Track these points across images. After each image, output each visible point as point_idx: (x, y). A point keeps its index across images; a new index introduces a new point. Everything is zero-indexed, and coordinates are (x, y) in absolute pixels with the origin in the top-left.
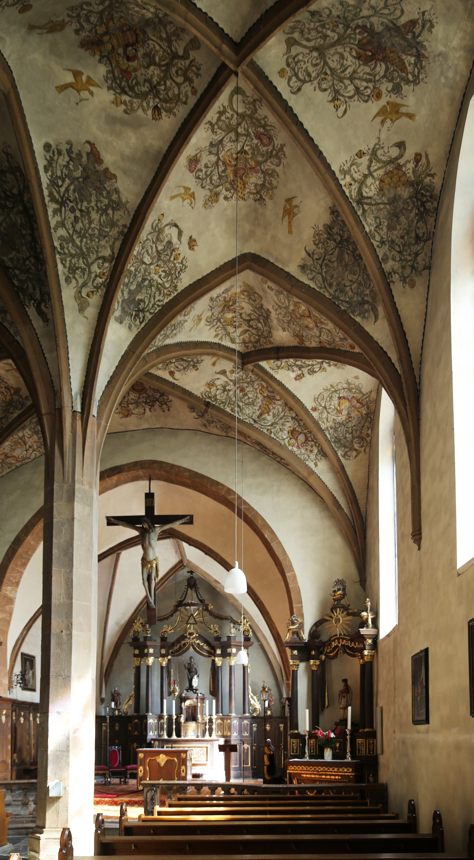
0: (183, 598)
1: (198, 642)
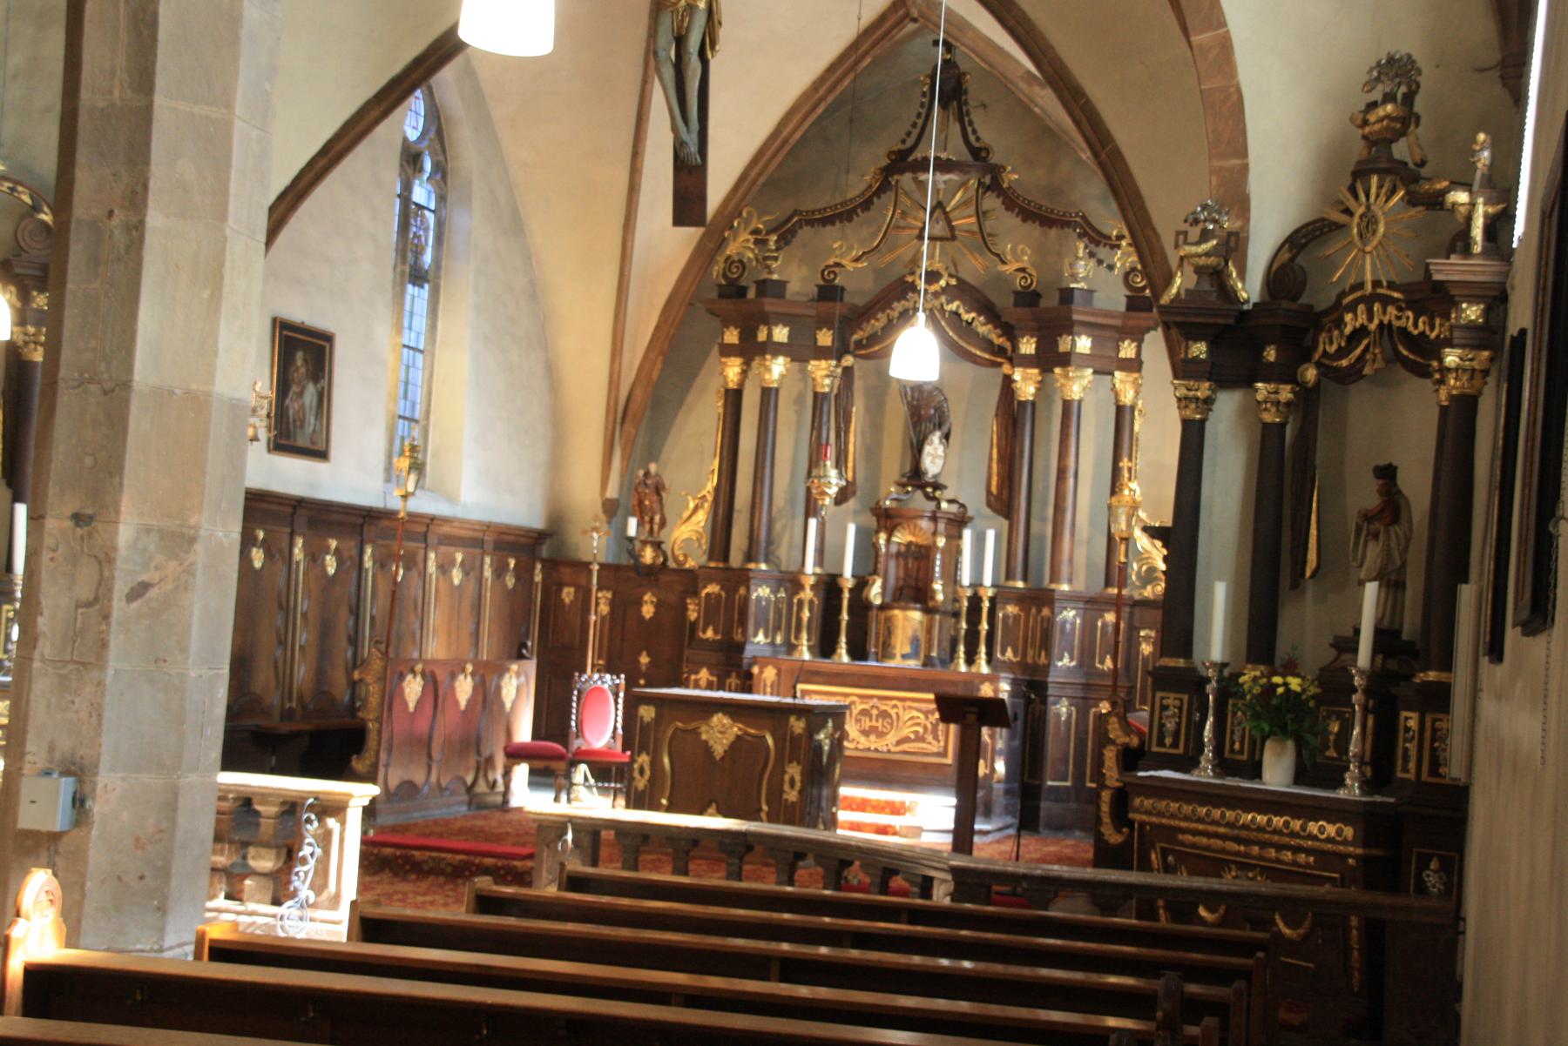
0: (910, 143)
1: (953, 306)
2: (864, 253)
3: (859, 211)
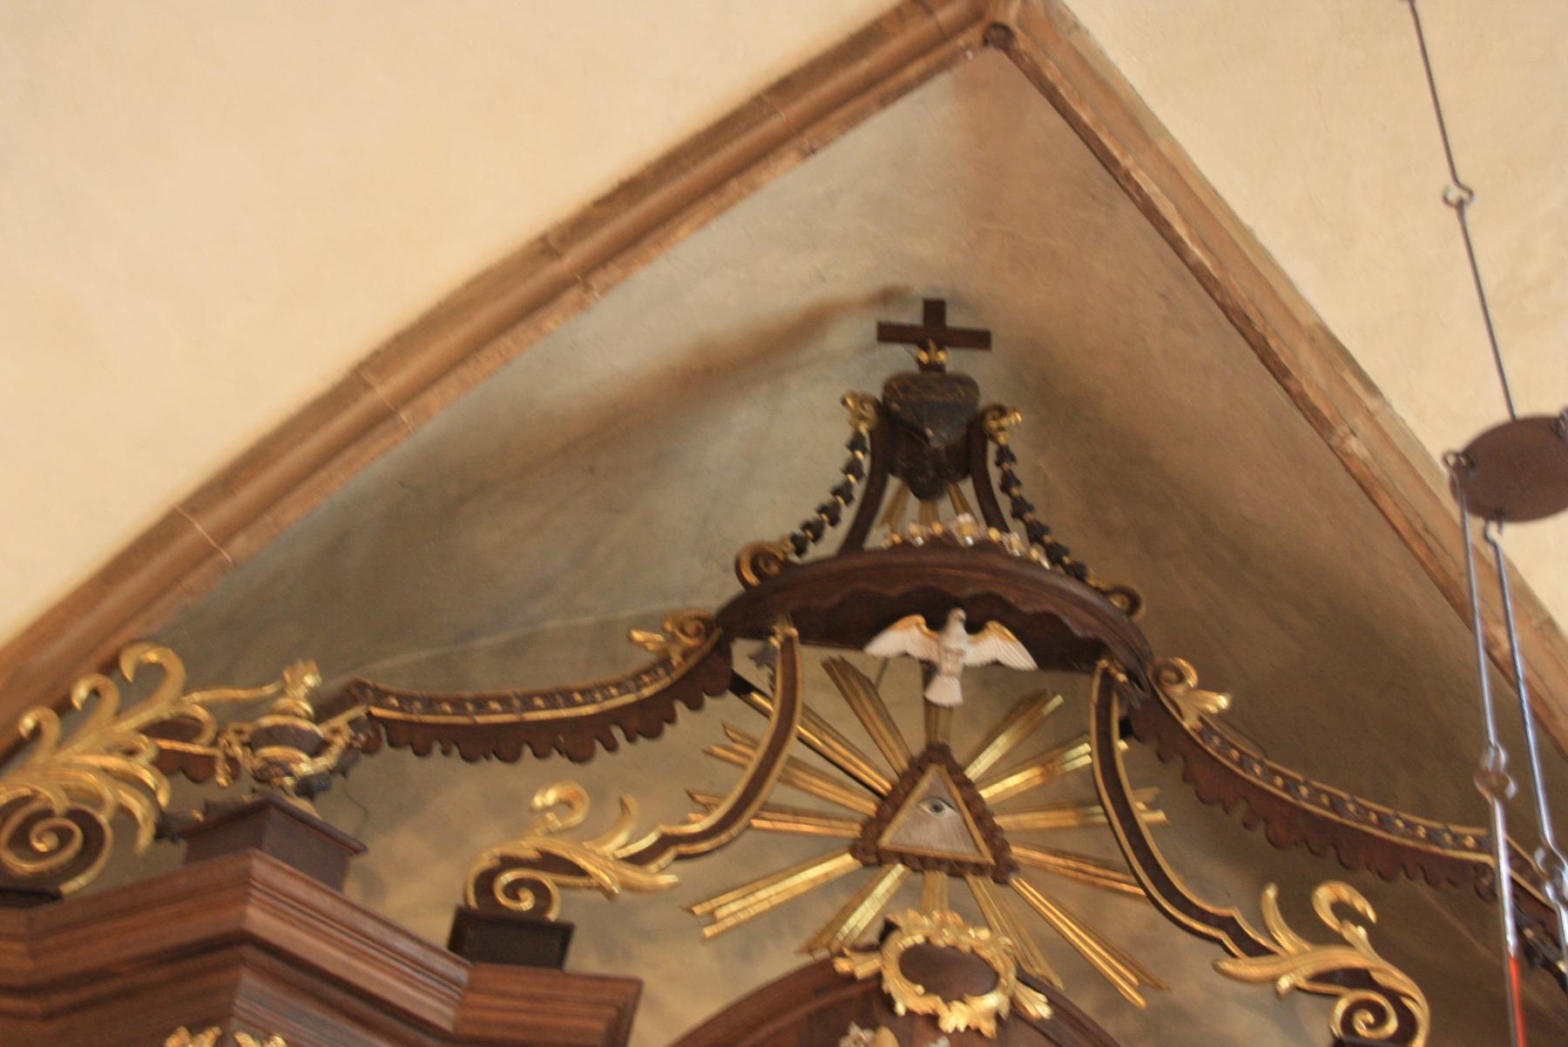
2: (665, 842)
3: (618, 733)
